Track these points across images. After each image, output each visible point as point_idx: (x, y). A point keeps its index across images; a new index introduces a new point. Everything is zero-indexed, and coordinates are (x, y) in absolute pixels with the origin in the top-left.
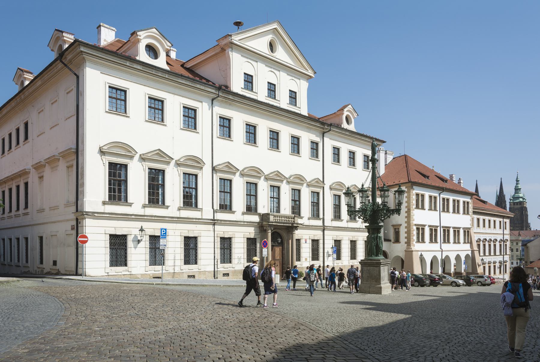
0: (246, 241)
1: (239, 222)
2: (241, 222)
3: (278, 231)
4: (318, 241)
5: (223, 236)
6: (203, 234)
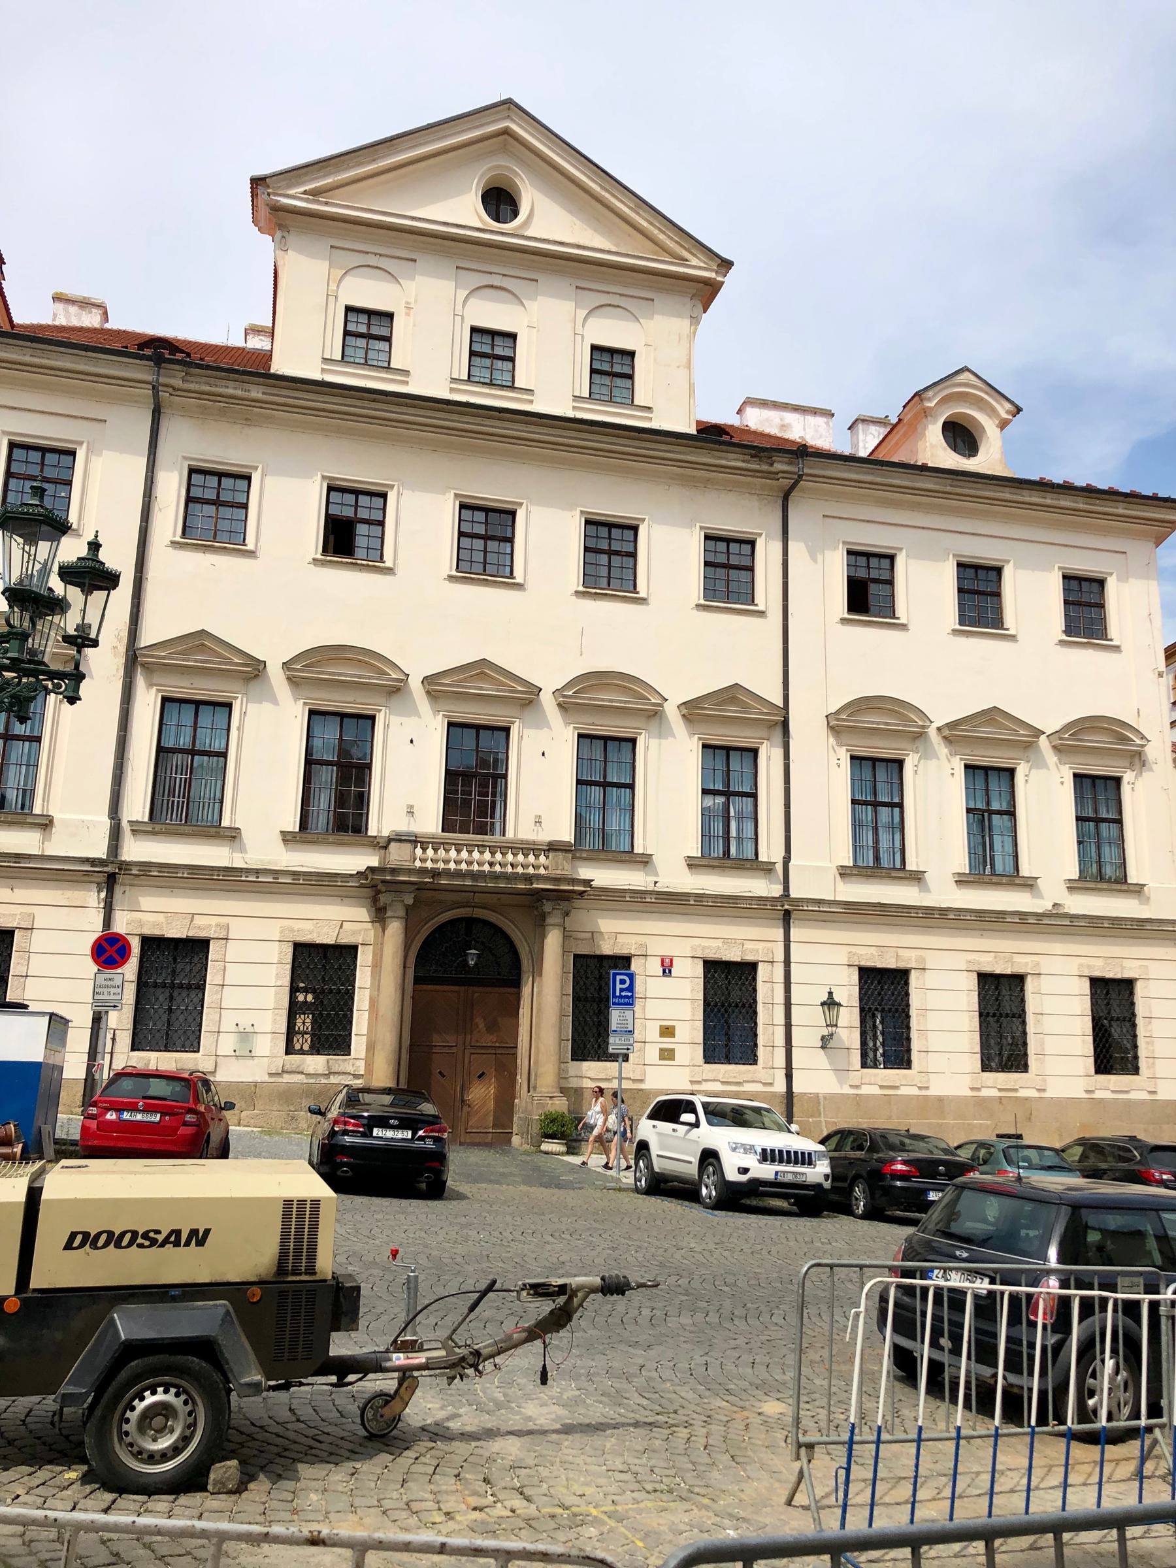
0: (289, 958)
1: (248, 871)
2: (257, 872)
4: (750, 968)
5: (157, 932)
6: (43, 918)
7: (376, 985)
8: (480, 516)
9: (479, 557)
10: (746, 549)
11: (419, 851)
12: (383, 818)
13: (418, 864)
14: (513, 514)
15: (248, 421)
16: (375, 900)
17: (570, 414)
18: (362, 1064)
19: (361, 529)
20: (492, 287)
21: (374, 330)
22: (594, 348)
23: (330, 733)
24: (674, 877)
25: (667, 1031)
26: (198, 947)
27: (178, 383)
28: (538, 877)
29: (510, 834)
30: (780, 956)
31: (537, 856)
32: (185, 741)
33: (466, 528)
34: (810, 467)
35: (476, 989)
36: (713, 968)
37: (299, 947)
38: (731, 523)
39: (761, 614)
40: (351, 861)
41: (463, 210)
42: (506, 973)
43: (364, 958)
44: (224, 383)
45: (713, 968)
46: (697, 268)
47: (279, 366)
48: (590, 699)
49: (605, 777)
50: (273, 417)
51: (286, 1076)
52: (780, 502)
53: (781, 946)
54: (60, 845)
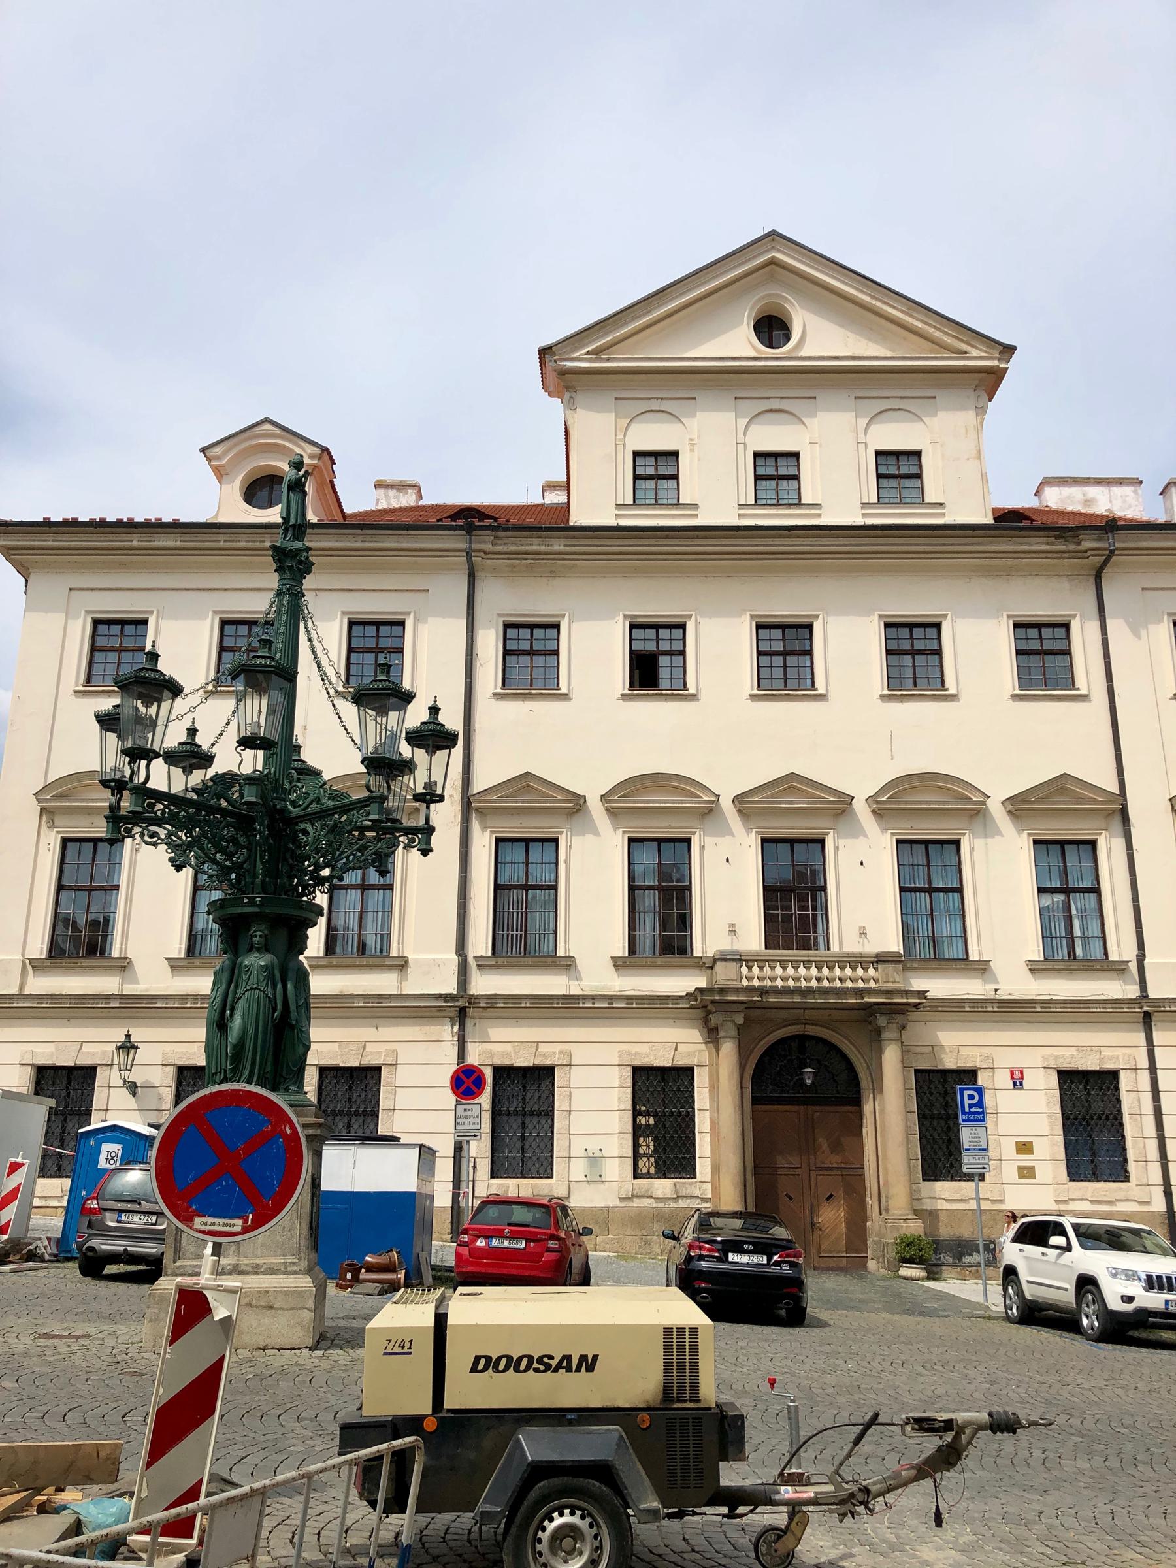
0: (629, 1082)
1: (585, 998)
2: (593, 998)
3: (811, 1030)
4: (1110, 1078)
5: (506, 1062)
6: (406, 1054)
7: (716, 1108)
8: (777, 634)
9: (778, 673)
10: (1061, 632)
11: (744, 970)
12: (707, 938)
13: (745, 983)
14: (810, 627)
15: (553, 573)
16: (706, 1020)
17: (860, 521)
18: (708, 1187)
19: (664, 661)
20: (771, 411)
21: (662, 471)
22: (878, 454)
23: (649, 858)
24: (1016, 982)
25: (1024, 1148)
26: (543, 1075)
27: (488, 547)
28: (869, 991)
29: (835, 947)
30: (1144, 1062)
31: (865, 969)
32: (518, 877)
33: (764, 647)
34: (1121, 541)
35: (817, 1108)
36: (1068, 1078)
37: (637, 1071)
38: (1041, 608)
39: (1084, 698)
40: (679, 983)
41: (737, 342)
42: (845, 1091)
43: (701, 1079)
44: (529, 541)
45: (1068, 1078)
46: (978, 357)
47: (578, 518)
48: (906, 803)
49: (930, 882)
50: (574, 566)
51: (635, 1200)
52: (1092, 580)
53: (1143, 1052)
54: (417, 984)
